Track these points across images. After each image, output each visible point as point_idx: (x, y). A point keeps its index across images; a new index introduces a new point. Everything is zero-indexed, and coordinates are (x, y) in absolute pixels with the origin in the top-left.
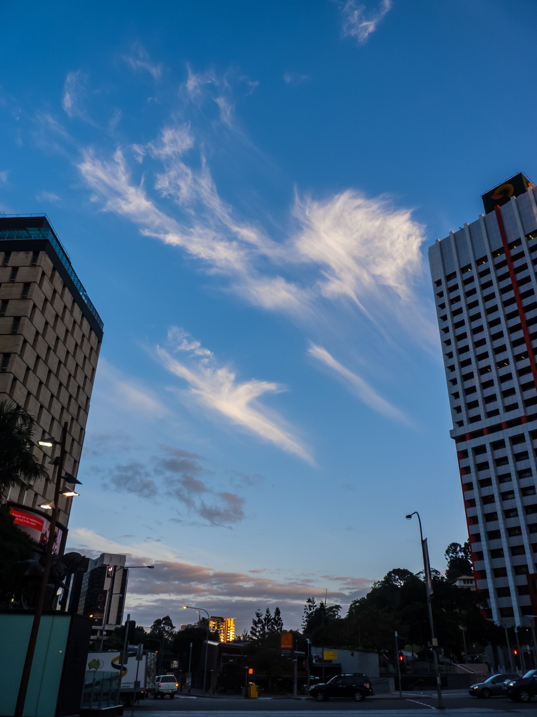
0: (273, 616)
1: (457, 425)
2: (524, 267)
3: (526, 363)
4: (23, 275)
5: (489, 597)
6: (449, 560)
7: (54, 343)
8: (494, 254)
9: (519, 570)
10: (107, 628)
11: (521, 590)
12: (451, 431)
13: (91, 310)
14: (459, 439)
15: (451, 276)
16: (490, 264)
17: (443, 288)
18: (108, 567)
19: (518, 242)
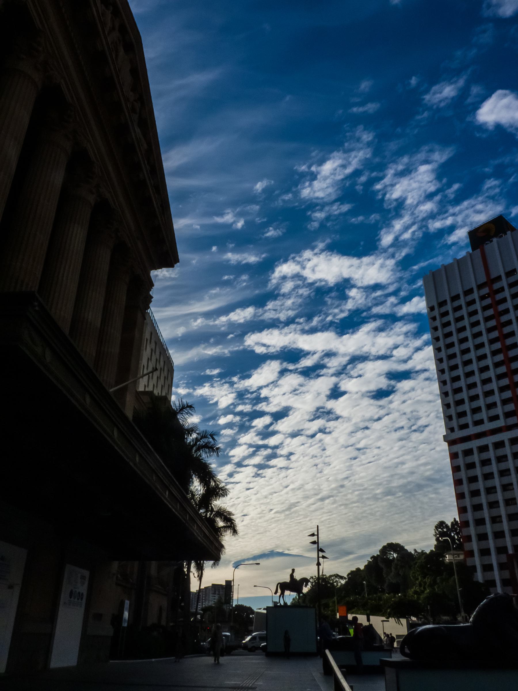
1: (449, 431)
2: (507, 311)
3: (508, 394)
8: (480, 287)
9: (501, 550)
11: (502, 567)
12: (444, 436)
14: (451, 443)
15: (442, 304)
16: (475, 295)
19: (499, 278)
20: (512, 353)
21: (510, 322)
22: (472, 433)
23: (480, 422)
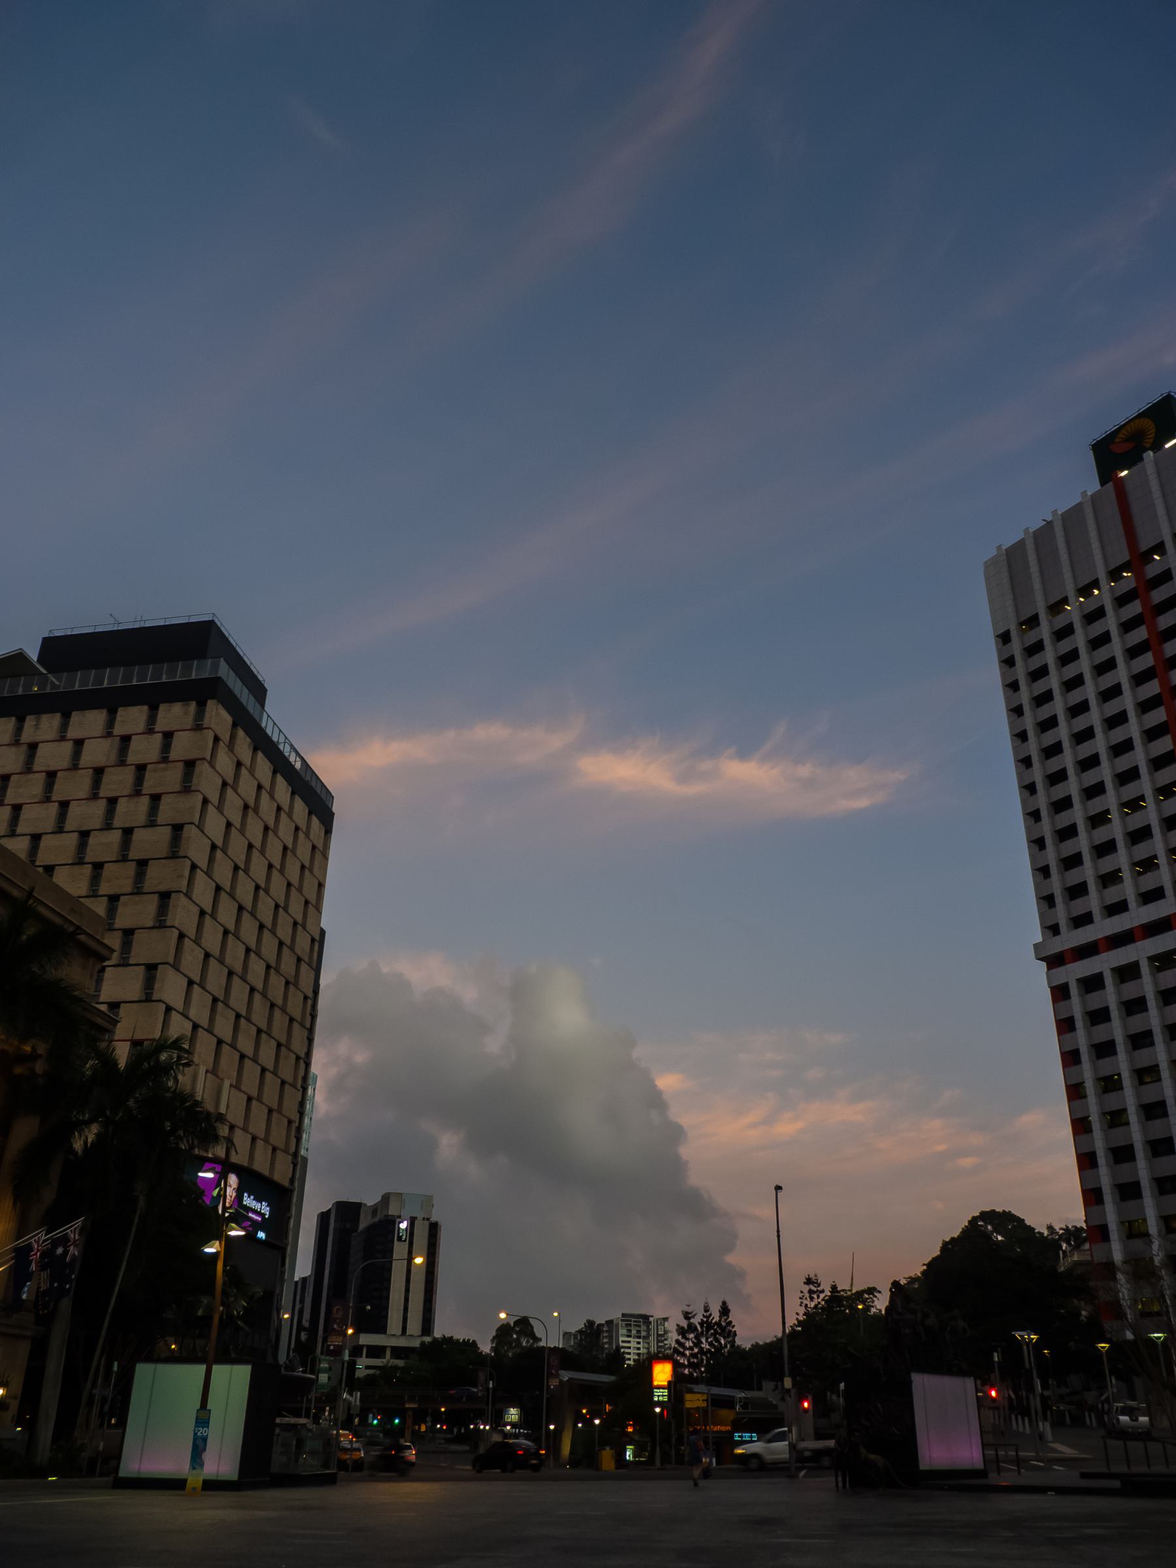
0: (717, 1319)
4: (182, 746)
7: (243, 858)
8: (1115, 574)
10: (402, 1342)
12: (1036, 946)
13: (308, 778)
14: (1054, 961)
17: (1016, 648)
23: (1120, 907)
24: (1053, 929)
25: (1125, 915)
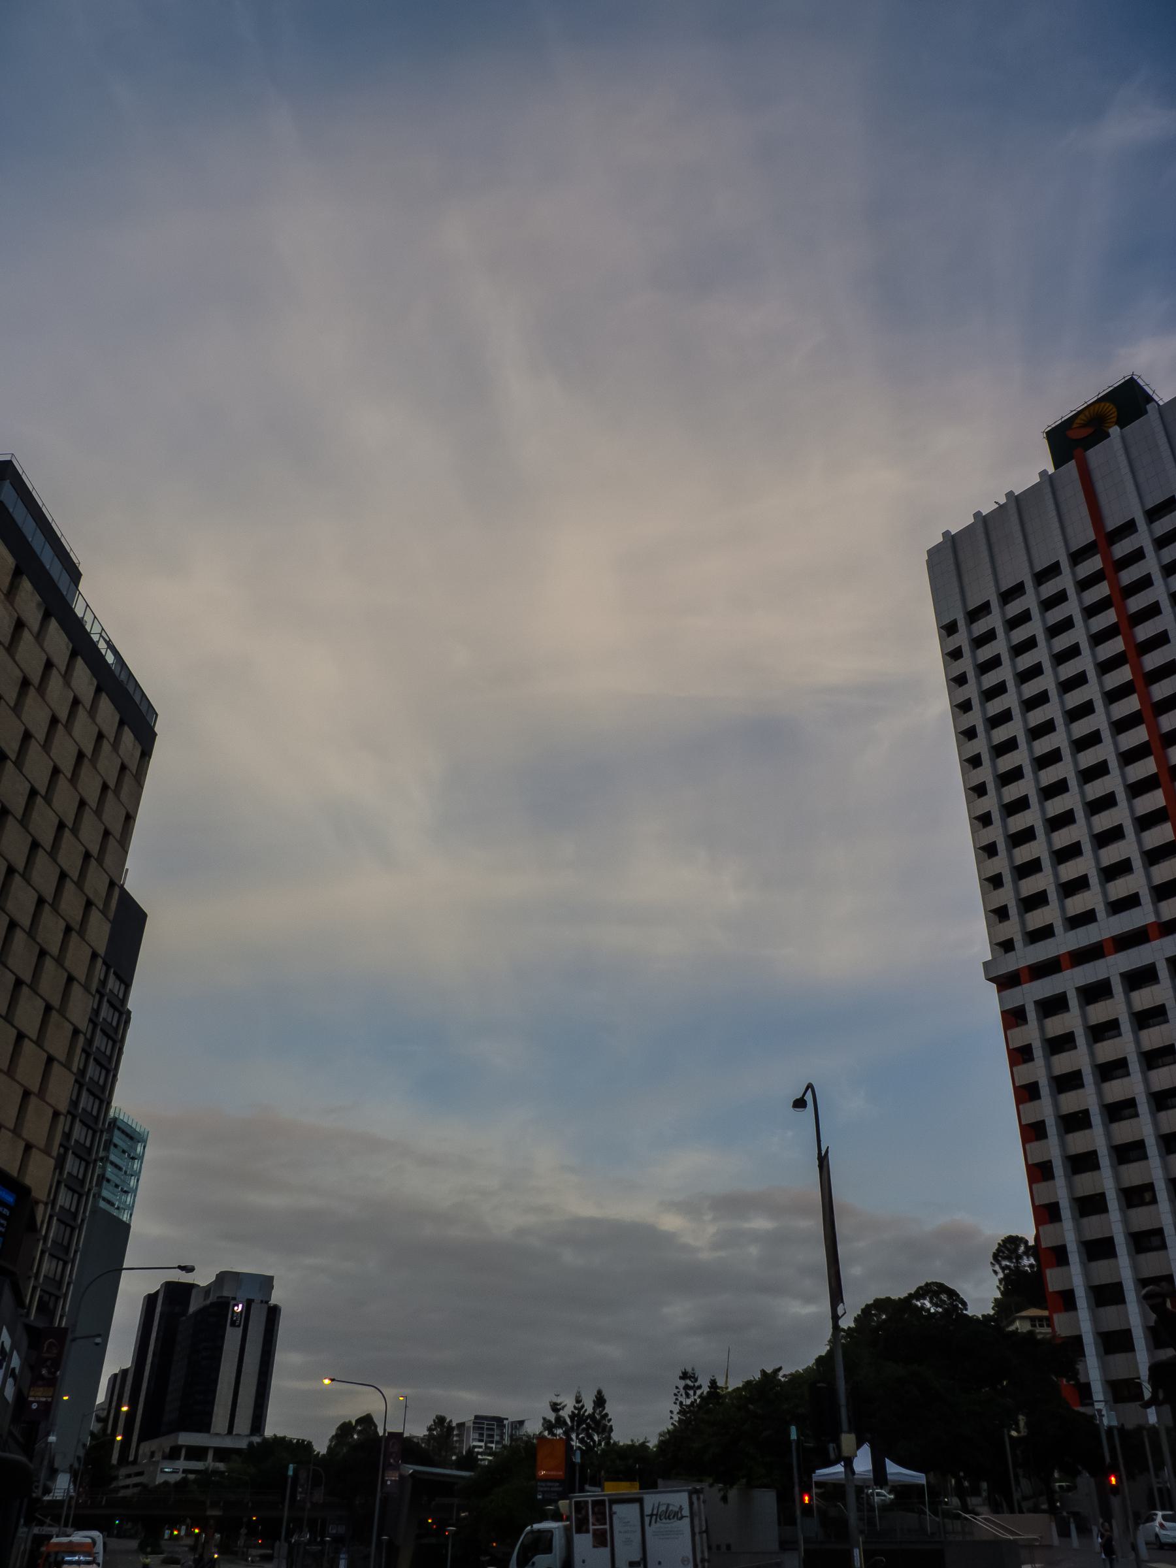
0: (590, 1411)
1: (1000, 951)
5: (1082, 1354)
6: (1001, 1275)
8: (1077, 557)
10: (228, 1443)
12: (986, 964)
13: (123, 677)
14: (1005, 982)
16: (1065, 581)
17: (961, 639)
18: (232, 1302)
19: (1129, 528)
20: (1161, 690)
21: (1153, 610)
22: (1063, 950)
24: (1007, 946)
25: (1092, 927)
